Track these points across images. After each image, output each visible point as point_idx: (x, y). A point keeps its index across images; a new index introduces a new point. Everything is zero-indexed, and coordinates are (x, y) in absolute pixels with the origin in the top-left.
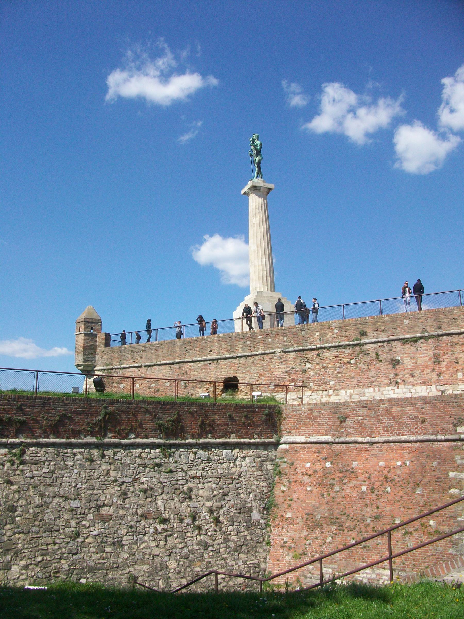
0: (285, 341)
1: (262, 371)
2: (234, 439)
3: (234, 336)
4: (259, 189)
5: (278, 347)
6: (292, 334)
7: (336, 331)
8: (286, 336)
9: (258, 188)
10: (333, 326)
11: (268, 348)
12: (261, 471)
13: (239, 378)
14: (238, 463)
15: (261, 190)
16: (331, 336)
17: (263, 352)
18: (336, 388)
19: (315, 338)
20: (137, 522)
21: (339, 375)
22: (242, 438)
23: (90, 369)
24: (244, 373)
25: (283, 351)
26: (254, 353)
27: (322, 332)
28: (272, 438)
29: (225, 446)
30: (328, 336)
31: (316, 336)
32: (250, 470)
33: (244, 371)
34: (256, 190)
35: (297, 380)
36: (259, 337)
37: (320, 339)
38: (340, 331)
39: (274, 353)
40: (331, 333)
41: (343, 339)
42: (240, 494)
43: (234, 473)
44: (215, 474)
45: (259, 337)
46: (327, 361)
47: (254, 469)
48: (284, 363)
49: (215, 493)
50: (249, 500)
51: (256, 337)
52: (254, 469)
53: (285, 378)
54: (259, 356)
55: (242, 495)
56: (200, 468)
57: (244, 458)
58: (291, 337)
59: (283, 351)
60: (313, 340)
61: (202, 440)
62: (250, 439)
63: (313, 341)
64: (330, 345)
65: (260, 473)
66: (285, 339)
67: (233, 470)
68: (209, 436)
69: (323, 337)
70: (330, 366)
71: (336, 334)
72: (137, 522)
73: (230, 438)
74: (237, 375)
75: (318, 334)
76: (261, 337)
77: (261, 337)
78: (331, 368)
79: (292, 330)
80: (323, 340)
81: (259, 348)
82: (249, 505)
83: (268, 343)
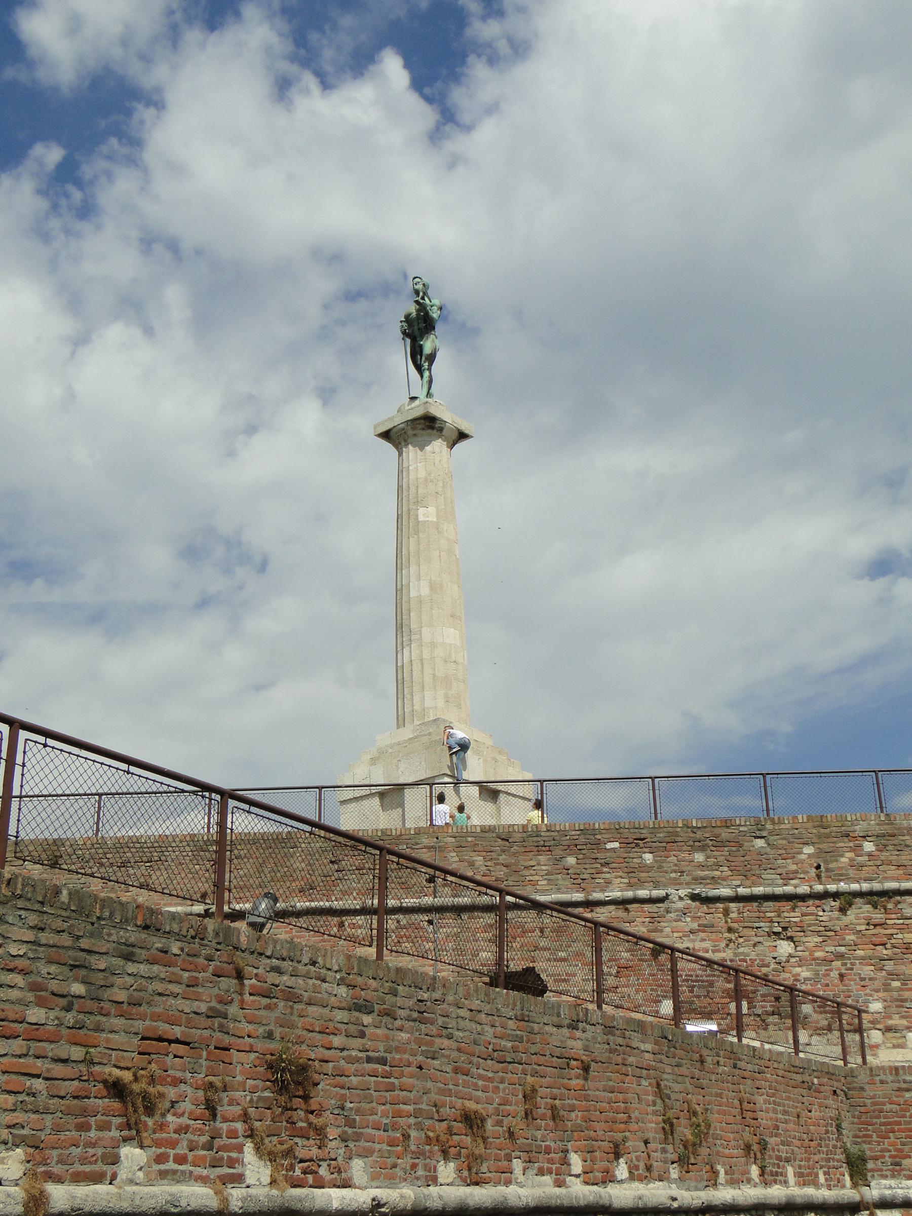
0: (701, 866)
1: (626, 955)
3: (518, 836)
4: (441, 430)
5: (677, 883)
6: (719, 844)
7: (869, 847)
8: (703, 849)
9: (437, 426)
10: (859, 829)
11: (641, 883)
13: (543, 976)
15: (445, 432)
16: (851, 860)
17: (630, 894)
18: (890, 1022)
19: (802, 861)
21: (896, 984)
24: (564, 960)
25: (694, 897)
26: (597, 896)
27: (824, 846)
30: (843, 860)
31: (803, 857)
33: (562, 954)
34: (432, 428)
35: (754, 992)
36: (610, 846)
37: (818, 867)
38: (882, 848)
39: (665, 898)
40: (852, 850)
41: (892, 871)
45: (610, 846)
46: (850, 938)
48: (702, 935)
51: (598, 845)
53: (711, 984)
54: (612, 907)
58: (721, 855)
59: (694, 897)
60: (794, 867)
63: (796, 872)
64: (855, 887)
66: (699, 857)
69: (826, 862)
70: (860, 953)
71: (870, 855)
74: (539, 966)
75: (809, 850)
76: (616, 845)
77: (616, 845)
78: (863, 958)
79: (725, 834)
80: (827, 870)
81: (608, 882)
83: (644, 868)
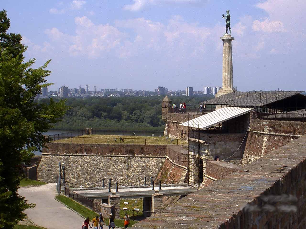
2: (151, 155)
12: (158, 165)
14: (150, 163)
20: (116, 176)
22: (154, 155)
23: (166, 120)
28: (164, 156)
29: (147, 157)
32: (154, 165)
42: (148, 171)
43: (148, 165)
44: (142, 165)
47: (155, 165)
49: (141, 171)
50: (150, 174)
52: (155, 165)
55: (149, 172)
56: (138, 163)
57: (153, 161)
61: (140, 156)
62: (156, 156)
65: (157, 166)
67: (148, 165)
68: (142, 154)
72: (116, 176)
73: (149, 155)
82: (150, 175)
